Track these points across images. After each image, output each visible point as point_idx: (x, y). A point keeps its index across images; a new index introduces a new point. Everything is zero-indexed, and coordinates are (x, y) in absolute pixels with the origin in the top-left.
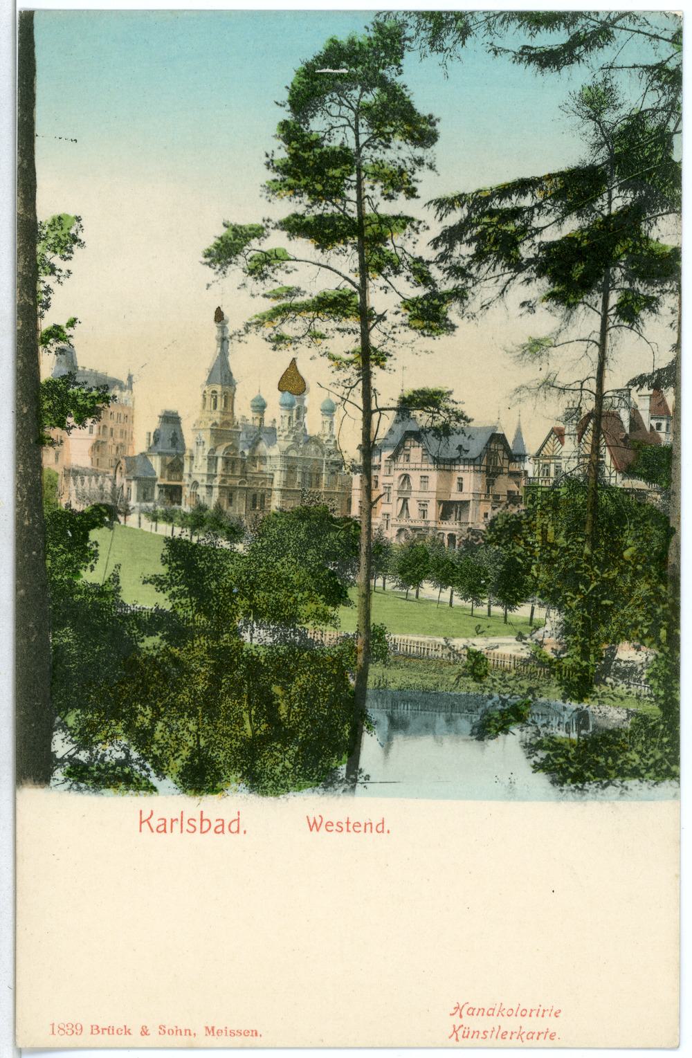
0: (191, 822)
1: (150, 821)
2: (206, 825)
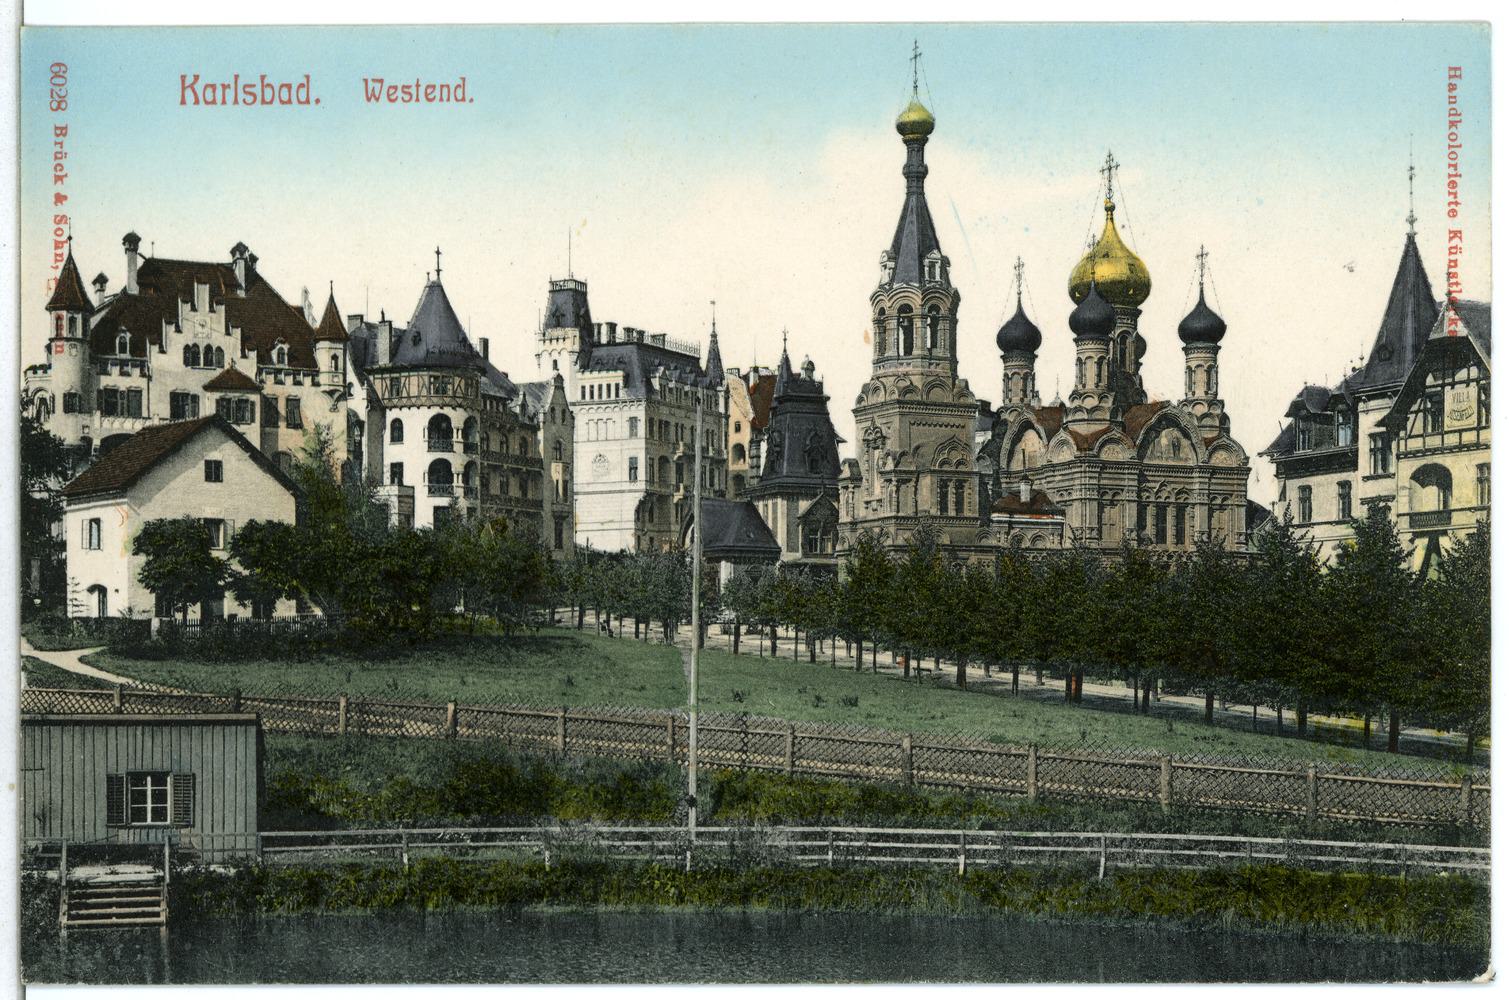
0: (247, 89)
1: (195, 86)
2: (268, 91)
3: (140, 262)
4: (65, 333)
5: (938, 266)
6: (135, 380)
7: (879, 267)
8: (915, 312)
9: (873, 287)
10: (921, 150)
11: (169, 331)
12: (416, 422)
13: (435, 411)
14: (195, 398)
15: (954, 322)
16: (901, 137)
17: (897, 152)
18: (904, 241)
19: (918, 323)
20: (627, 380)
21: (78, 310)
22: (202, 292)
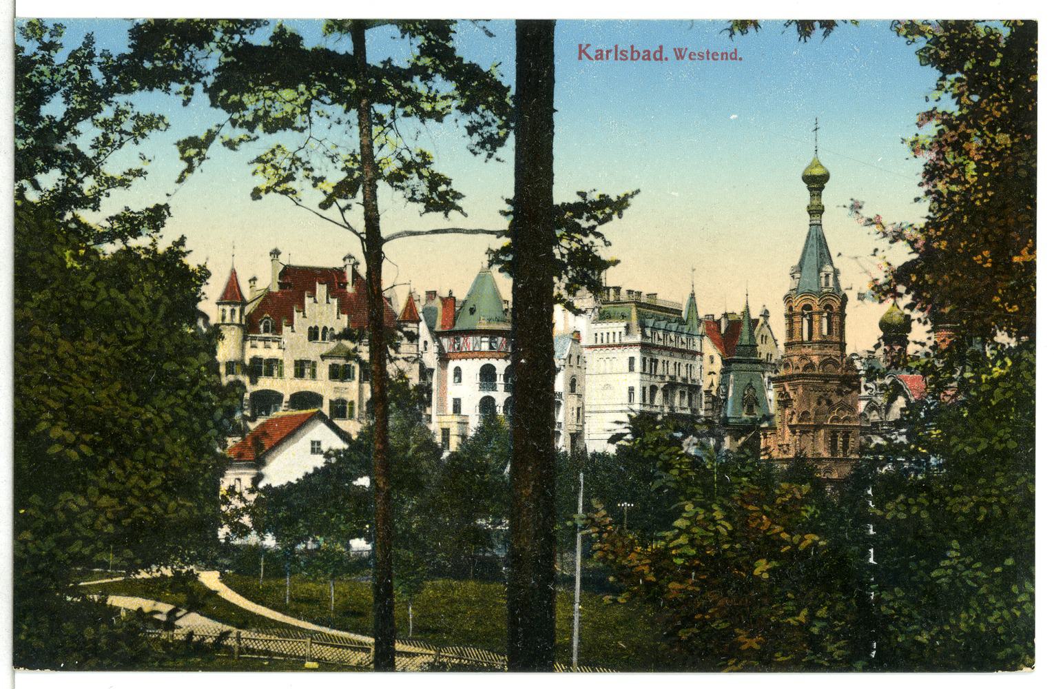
3: (281, 268)
4: (227, 320)
5: (831, 276)
6: (273, 352)
7: (789, 277)
8: (814, 309)
9: (786, 291)
10: (820, 195)
11: (297, 316)
12: (471, 368)
13: (485, 361)
14: (314, 364)
15: (843, 316)
16: (805, 185)
17: (803, 194)
18: (807, 257)
19: (816, 317)
20: (627, 328)
21: (236, 304)
22: (321, 290)
